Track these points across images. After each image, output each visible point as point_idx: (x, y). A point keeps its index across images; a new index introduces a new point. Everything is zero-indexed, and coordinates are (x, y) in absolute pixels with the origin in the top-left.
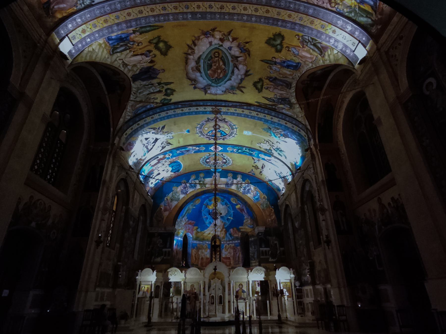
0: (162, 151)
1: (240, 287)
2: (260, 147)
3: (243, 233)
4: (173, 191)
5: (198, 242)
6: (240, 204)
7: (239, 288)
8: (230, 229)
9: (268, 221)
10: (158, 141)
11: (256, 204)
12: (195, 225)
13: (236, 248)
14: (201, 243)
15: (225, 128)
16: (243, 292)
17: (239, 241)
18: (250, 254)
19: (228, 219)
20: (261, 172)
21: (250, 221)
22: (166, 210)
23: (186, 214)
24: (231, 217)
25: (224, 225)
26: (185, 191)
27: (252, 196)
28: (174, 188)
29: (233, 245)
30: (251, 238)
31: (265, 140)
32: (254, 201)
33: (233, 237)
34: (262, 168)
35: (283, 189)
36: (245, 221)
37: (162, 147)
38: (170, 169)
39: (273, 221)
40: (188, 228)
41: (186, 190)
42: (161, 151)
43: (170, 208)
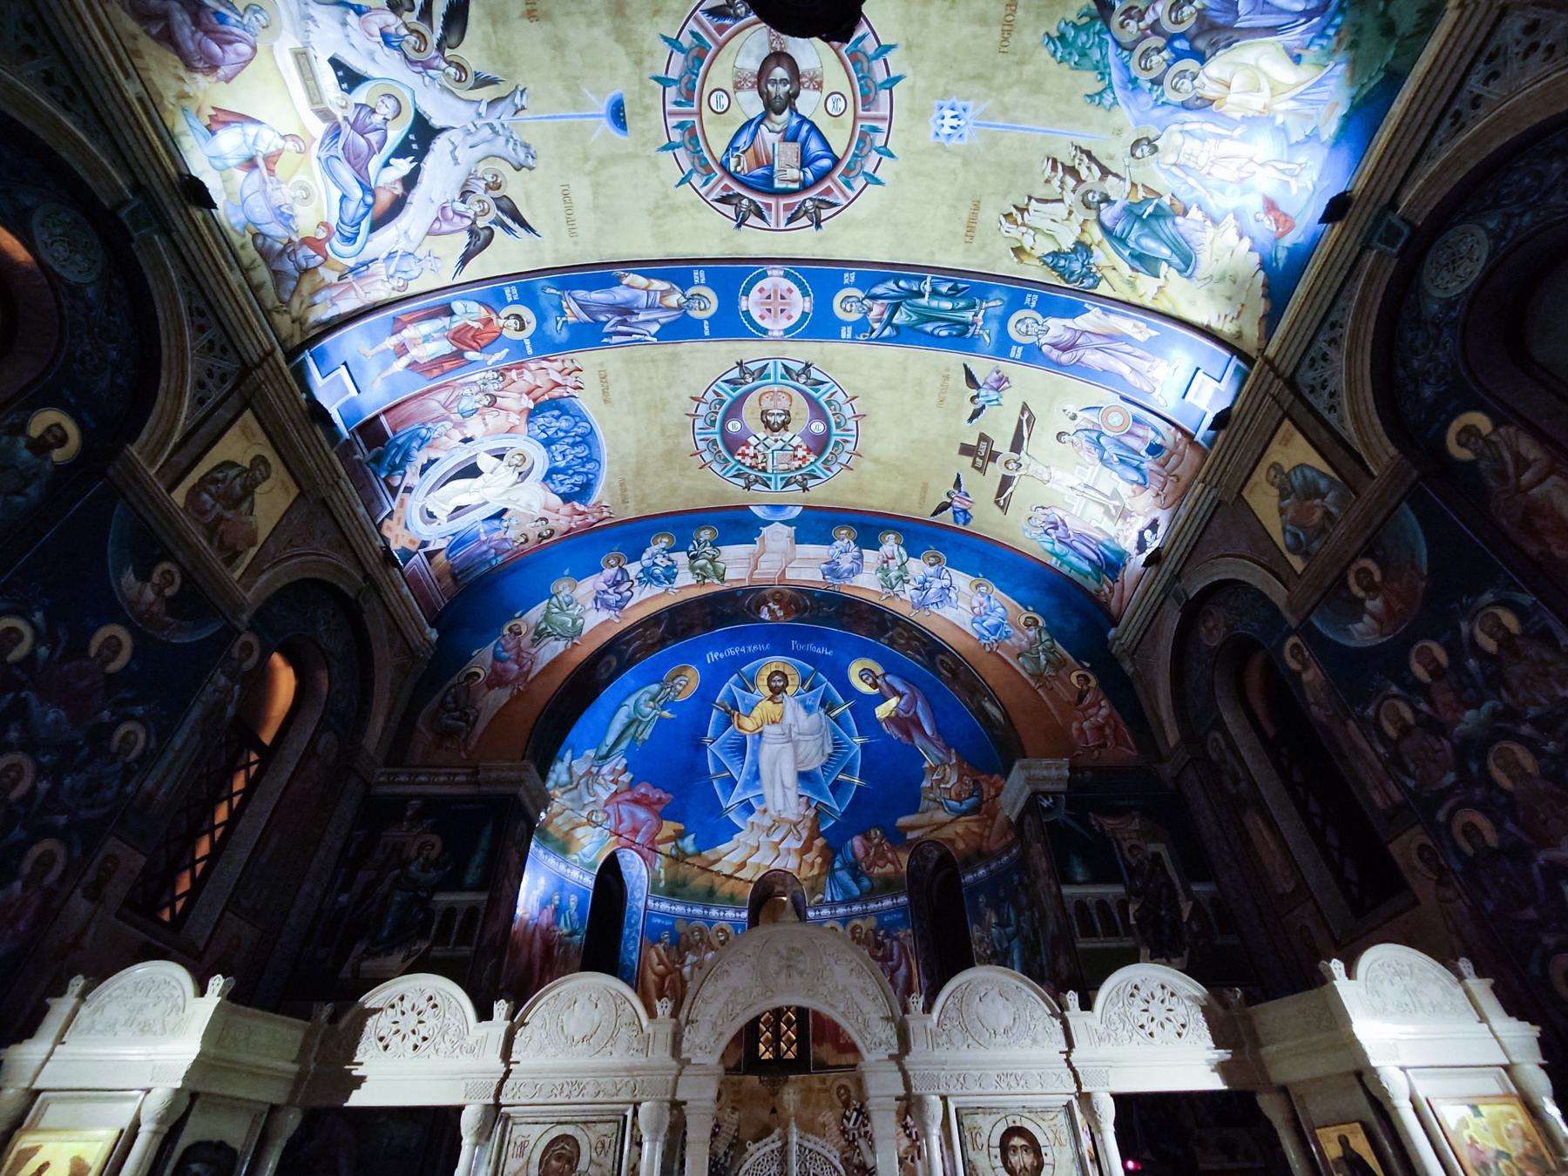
0: (474, 270)
2: (1018, 251)
3: (917, 849)
5: (679, 909)
6: (896, 693)
9: (1075, 733)
10: (440, 145)
13: (887, 941)
14: (696, 917)
15: (826, 92)
17: (903, 899)
19: (836, 787)
20: (1006, 482)
21: (954, 779)
22: (497, 679)
23: (624, 745)
25: (820, 814)
26: (612, 598)
27: (968, 617)
28: (562, 588)
29: (872, 922)
31: (1055, 161)
33: (866, 883)
34: (1017, 446)
35: (1148, 534)
36: (926, 784)
37: (473, 232)
38: (540, 459)
39: (1108, 731)
40: (625, 826)
41: (620, 594)
42: (465, 259)
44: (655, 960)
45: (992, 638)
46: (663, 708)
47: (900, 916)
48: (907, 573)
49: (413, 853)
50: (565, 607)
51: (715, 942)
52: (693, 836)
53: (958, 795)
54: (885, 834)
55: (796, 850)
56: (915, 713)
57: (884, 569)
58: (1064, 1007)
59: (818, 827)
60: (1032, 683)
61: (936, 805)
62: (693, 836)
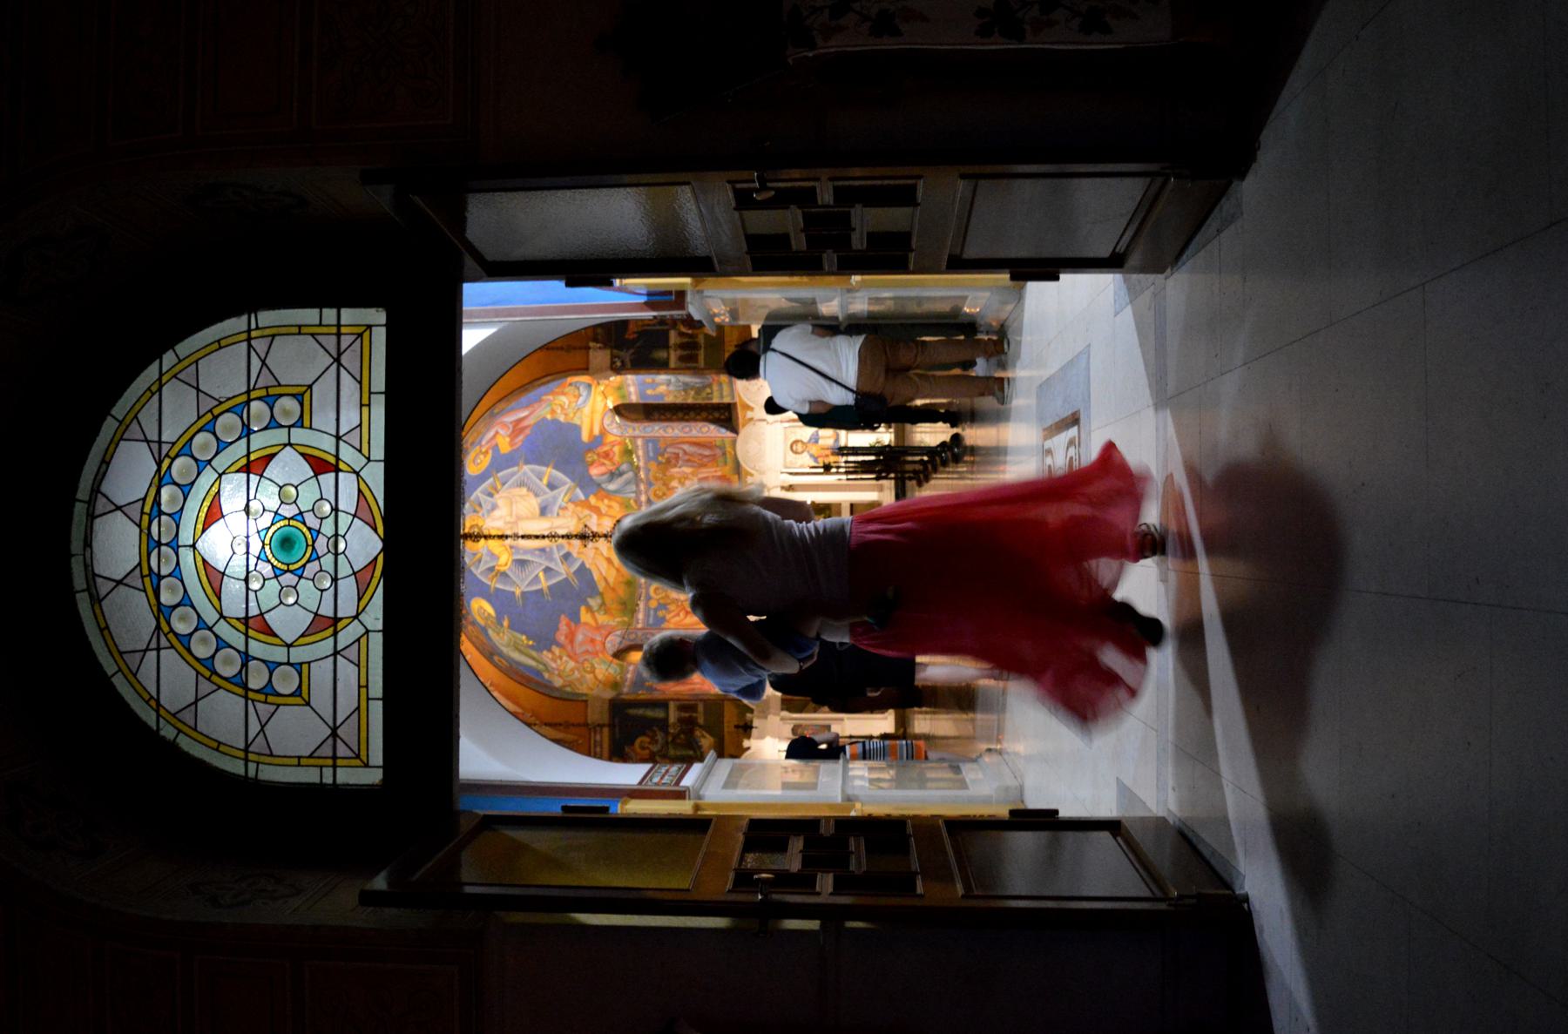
1: (800, 449)
7: (805, 454)
8: (590, 476)
12: (575, 617)
13: (666, 456)
16: (815, 440)
18: (690, 401)
19: (552, 486)
21: (564, 399)
24: (544, 474)
29: (653, 465)
30: (630, 393)
33: (624, 467)
36: (562, 418)
44: (677, 619)
46: (502, 625)
47: (650, 445)
49: (647, 752)
53: (575, 396)
55: (598, 519)
56: (511, 423)
58: (751, 419)
59: (581, 501)
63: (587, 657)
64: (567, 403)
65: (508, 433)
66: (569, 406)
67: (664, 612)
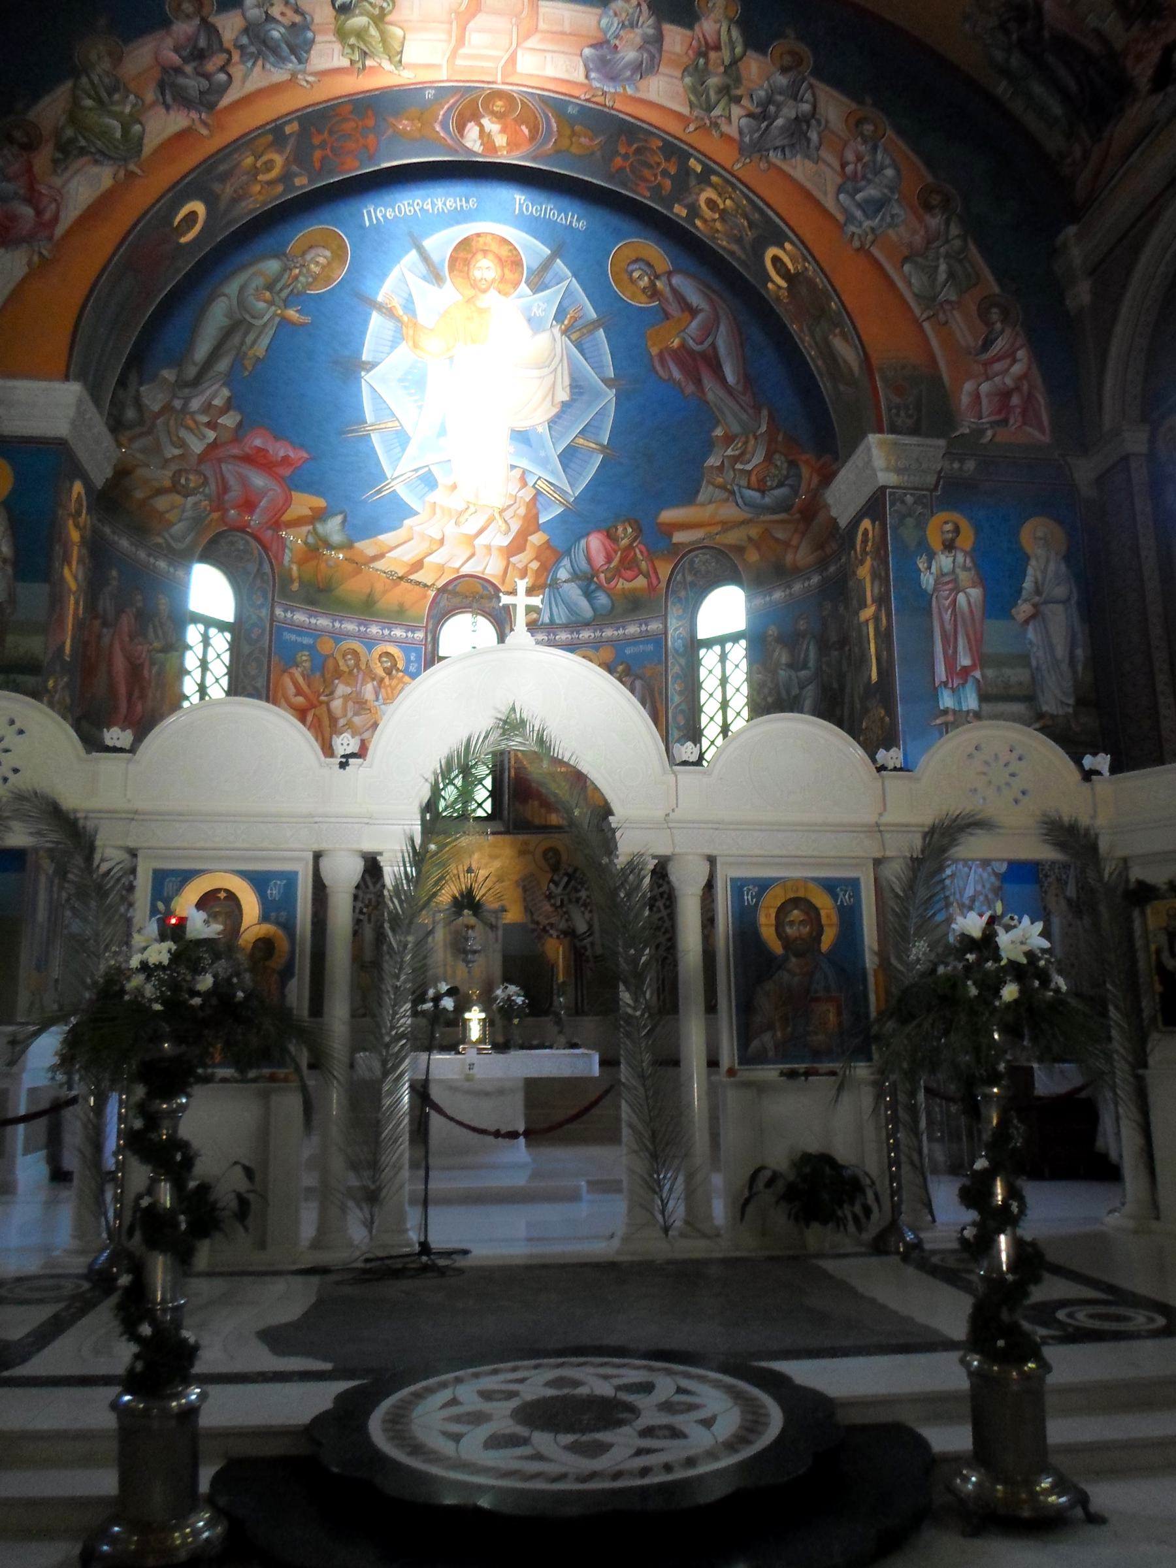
4: (75, 72)
8: (588, 535)
9: (965, 400)
11: (861, 249)
14: (349, 635)
21: (758, 458)
23: (223, 365)
32: (850, 218)
36: (713, 461)
39: (1015, 400)
41: (207, 76)
43: (48, 216)
44: (291, 690)
45: (867, 224)
47: (650, 647)
48: (738, 81)
50: (104, 95)
51: (380, 672)
52: (338, 519)
53: (762, 481)
54: (639, 530)
55: (500, 549)
56: (713, 346)
57: (697, 71)
59: (536, 517)
60: (917, 311)
61: (726, 495)
62: (338, 519)
63: (213, 487)
64: (749, 467)
65: (691, 342)
66: (742, 471)
67: (307, 664)
